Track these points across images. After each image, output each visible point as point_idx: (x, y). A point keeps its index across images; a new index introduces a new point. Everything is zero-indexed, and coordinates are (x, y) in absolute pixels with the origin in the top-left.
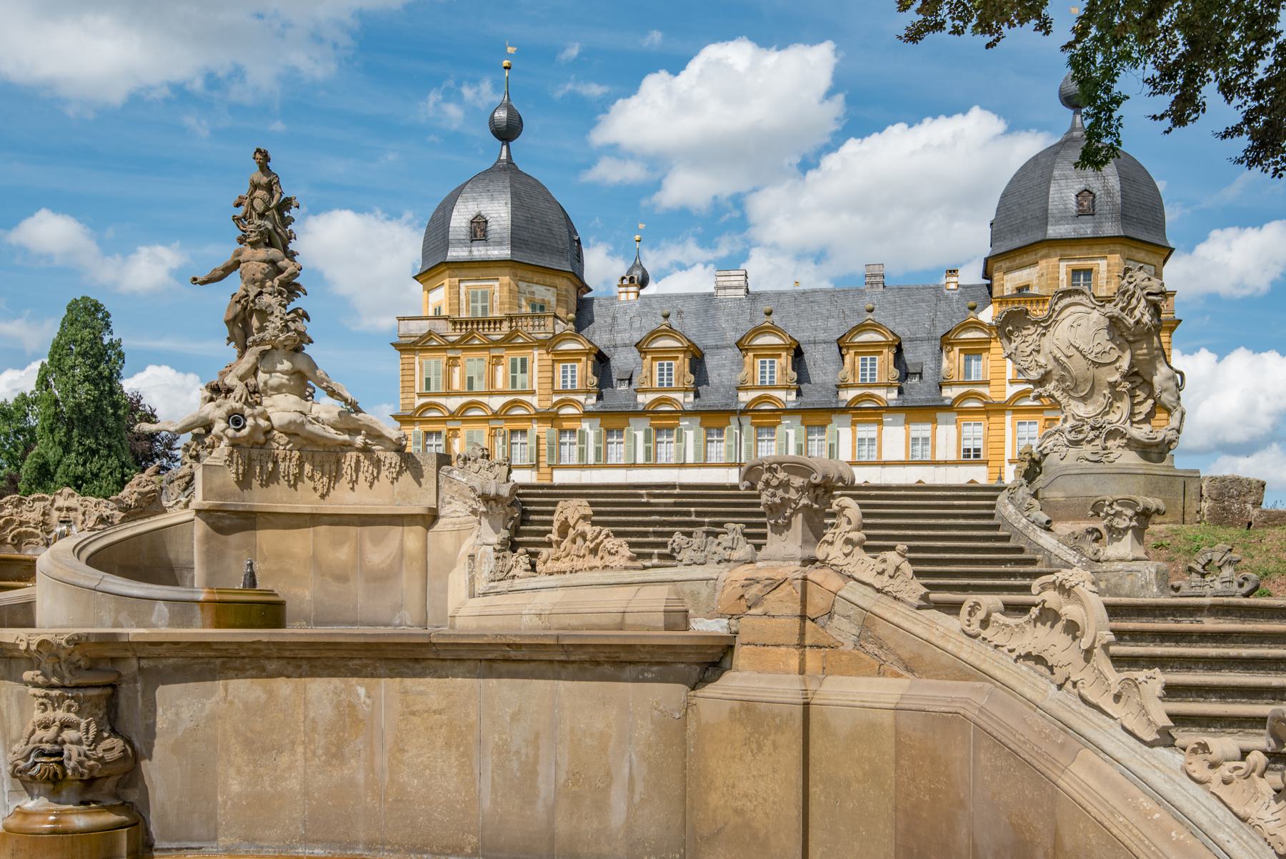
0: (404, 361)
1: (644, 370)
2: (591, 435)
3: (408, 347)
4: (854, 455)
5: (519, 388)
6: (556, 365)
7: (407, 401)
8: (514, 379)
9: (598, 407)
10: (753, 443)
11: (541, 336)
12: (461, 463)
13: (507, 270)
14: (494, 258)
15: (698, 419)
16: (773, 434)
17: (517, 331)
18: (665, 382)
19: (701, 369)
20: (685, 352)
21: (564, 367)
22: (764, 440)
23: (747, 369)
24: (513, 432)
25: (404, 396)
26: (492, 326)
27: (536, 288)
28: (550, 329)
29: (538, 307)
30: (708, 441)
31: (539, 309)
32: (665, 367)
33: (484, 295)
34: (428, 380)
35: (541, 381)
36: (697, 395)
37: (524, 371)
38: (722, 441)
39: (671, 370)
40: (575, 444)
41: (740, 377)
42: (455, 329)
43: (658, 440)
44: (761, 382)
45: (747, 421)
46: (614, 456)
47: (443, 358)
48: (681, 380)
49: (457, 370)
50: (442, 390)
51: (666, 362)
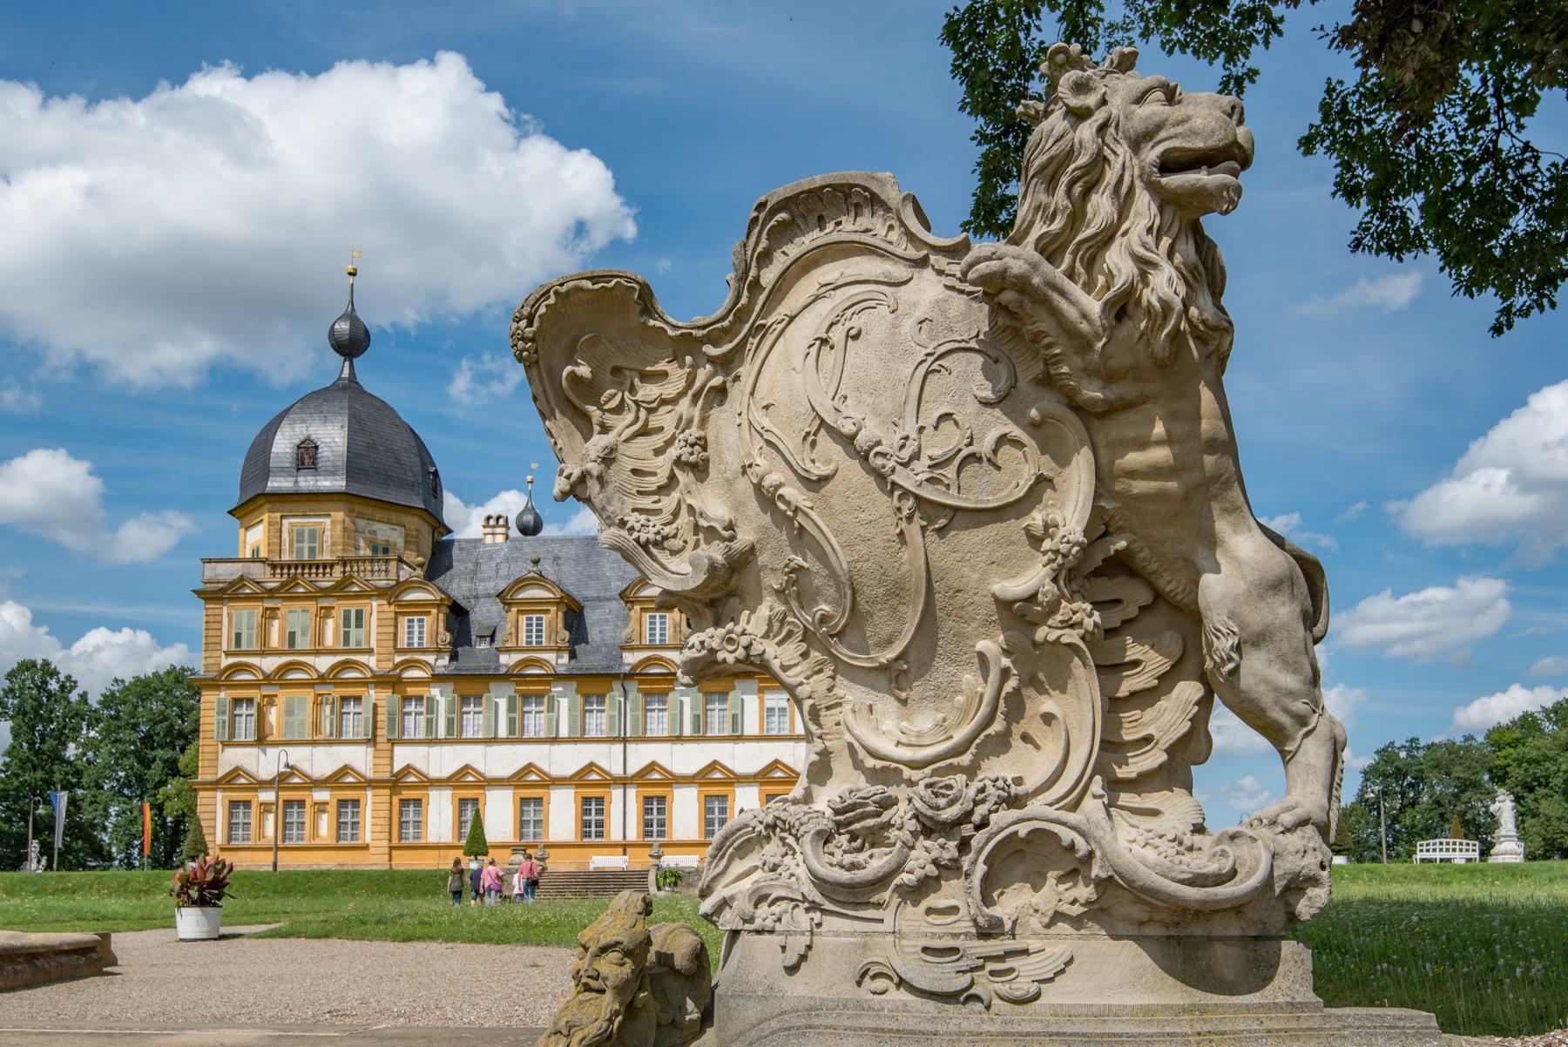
0: (209, 612)
1: (508, 626)
2: (442, 703)
3: (214, 595)
4: (761, 728)
5: (353, 645)
6: (400, 618)
7: (212, 661)
8: (347, 635)
9: (452, 669)
10: (640, 713)
11: (382, 583)
13: (340, 505)
14: (323, 490)
15: (574, 685)
16: (664, 703)
17: (352, 577)
18: (534, 639)
19: (579, 625)
20: (558, 604)
21: (409, 621)
22: (654, 710)
23: (633, 625)
24: (345, 699)
25: (208, 654)
26: (321, 570)
27: (377, 526)
28: (392, 575)
29: (380, 549)
30: (586, 711)
31: (382, 551)
32: (534, 622)
33: (313, 534)
34: (238, 636)
35: (381, 637)
36: (573, 656)
37: (359, 625)
38: (603, 711)
39: (541, 625)
40: (421, 713)
41: (625, 633)
42: (274, 574)
43: (526, 709)
45: (632, 686)
46: (470, 728)
47: (258, 608)
48: (553, 638)
49: (276, 623)
50: (256, 647)
51: (534, 616)
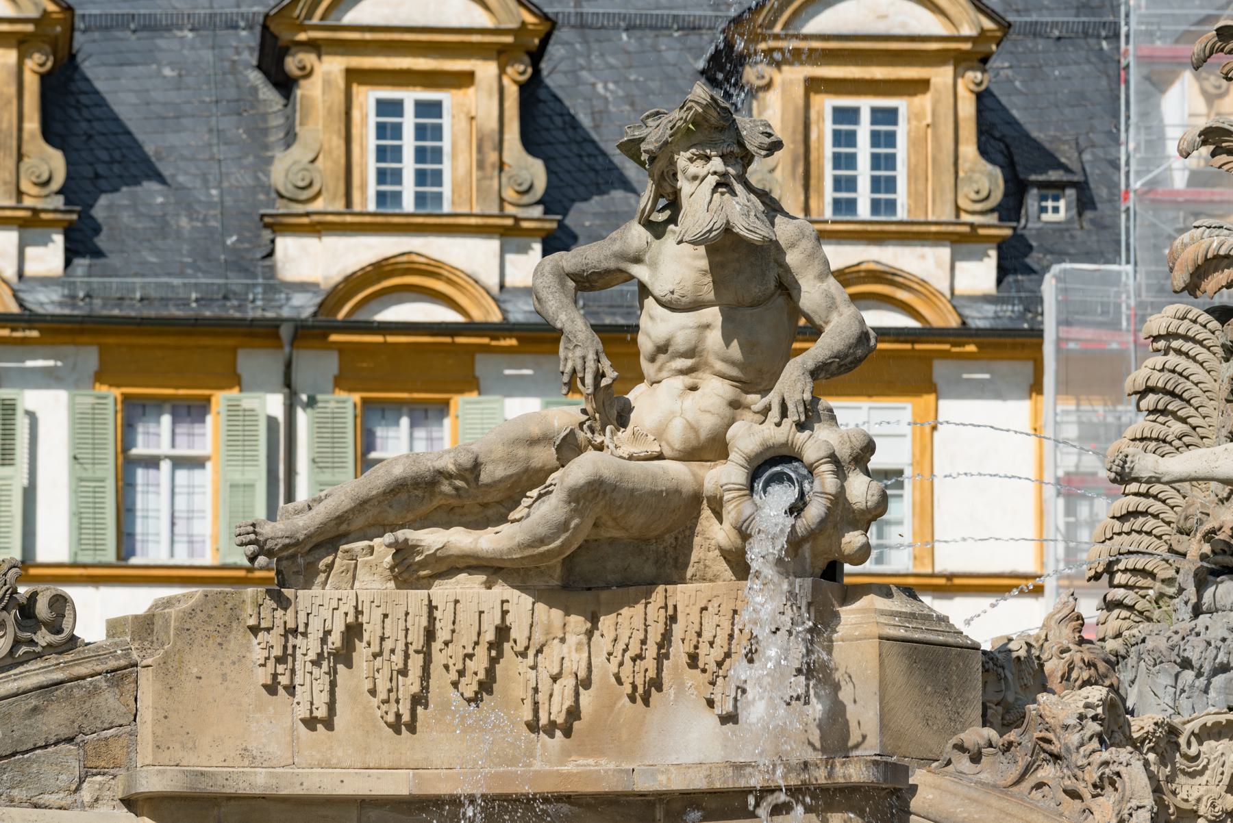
12: (367, 569)
44: (381, 197)
